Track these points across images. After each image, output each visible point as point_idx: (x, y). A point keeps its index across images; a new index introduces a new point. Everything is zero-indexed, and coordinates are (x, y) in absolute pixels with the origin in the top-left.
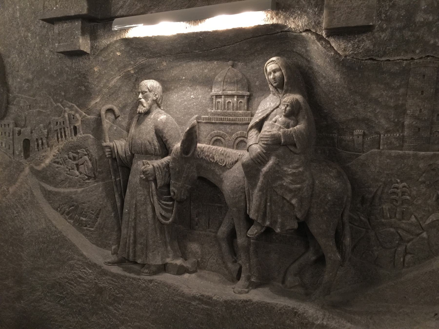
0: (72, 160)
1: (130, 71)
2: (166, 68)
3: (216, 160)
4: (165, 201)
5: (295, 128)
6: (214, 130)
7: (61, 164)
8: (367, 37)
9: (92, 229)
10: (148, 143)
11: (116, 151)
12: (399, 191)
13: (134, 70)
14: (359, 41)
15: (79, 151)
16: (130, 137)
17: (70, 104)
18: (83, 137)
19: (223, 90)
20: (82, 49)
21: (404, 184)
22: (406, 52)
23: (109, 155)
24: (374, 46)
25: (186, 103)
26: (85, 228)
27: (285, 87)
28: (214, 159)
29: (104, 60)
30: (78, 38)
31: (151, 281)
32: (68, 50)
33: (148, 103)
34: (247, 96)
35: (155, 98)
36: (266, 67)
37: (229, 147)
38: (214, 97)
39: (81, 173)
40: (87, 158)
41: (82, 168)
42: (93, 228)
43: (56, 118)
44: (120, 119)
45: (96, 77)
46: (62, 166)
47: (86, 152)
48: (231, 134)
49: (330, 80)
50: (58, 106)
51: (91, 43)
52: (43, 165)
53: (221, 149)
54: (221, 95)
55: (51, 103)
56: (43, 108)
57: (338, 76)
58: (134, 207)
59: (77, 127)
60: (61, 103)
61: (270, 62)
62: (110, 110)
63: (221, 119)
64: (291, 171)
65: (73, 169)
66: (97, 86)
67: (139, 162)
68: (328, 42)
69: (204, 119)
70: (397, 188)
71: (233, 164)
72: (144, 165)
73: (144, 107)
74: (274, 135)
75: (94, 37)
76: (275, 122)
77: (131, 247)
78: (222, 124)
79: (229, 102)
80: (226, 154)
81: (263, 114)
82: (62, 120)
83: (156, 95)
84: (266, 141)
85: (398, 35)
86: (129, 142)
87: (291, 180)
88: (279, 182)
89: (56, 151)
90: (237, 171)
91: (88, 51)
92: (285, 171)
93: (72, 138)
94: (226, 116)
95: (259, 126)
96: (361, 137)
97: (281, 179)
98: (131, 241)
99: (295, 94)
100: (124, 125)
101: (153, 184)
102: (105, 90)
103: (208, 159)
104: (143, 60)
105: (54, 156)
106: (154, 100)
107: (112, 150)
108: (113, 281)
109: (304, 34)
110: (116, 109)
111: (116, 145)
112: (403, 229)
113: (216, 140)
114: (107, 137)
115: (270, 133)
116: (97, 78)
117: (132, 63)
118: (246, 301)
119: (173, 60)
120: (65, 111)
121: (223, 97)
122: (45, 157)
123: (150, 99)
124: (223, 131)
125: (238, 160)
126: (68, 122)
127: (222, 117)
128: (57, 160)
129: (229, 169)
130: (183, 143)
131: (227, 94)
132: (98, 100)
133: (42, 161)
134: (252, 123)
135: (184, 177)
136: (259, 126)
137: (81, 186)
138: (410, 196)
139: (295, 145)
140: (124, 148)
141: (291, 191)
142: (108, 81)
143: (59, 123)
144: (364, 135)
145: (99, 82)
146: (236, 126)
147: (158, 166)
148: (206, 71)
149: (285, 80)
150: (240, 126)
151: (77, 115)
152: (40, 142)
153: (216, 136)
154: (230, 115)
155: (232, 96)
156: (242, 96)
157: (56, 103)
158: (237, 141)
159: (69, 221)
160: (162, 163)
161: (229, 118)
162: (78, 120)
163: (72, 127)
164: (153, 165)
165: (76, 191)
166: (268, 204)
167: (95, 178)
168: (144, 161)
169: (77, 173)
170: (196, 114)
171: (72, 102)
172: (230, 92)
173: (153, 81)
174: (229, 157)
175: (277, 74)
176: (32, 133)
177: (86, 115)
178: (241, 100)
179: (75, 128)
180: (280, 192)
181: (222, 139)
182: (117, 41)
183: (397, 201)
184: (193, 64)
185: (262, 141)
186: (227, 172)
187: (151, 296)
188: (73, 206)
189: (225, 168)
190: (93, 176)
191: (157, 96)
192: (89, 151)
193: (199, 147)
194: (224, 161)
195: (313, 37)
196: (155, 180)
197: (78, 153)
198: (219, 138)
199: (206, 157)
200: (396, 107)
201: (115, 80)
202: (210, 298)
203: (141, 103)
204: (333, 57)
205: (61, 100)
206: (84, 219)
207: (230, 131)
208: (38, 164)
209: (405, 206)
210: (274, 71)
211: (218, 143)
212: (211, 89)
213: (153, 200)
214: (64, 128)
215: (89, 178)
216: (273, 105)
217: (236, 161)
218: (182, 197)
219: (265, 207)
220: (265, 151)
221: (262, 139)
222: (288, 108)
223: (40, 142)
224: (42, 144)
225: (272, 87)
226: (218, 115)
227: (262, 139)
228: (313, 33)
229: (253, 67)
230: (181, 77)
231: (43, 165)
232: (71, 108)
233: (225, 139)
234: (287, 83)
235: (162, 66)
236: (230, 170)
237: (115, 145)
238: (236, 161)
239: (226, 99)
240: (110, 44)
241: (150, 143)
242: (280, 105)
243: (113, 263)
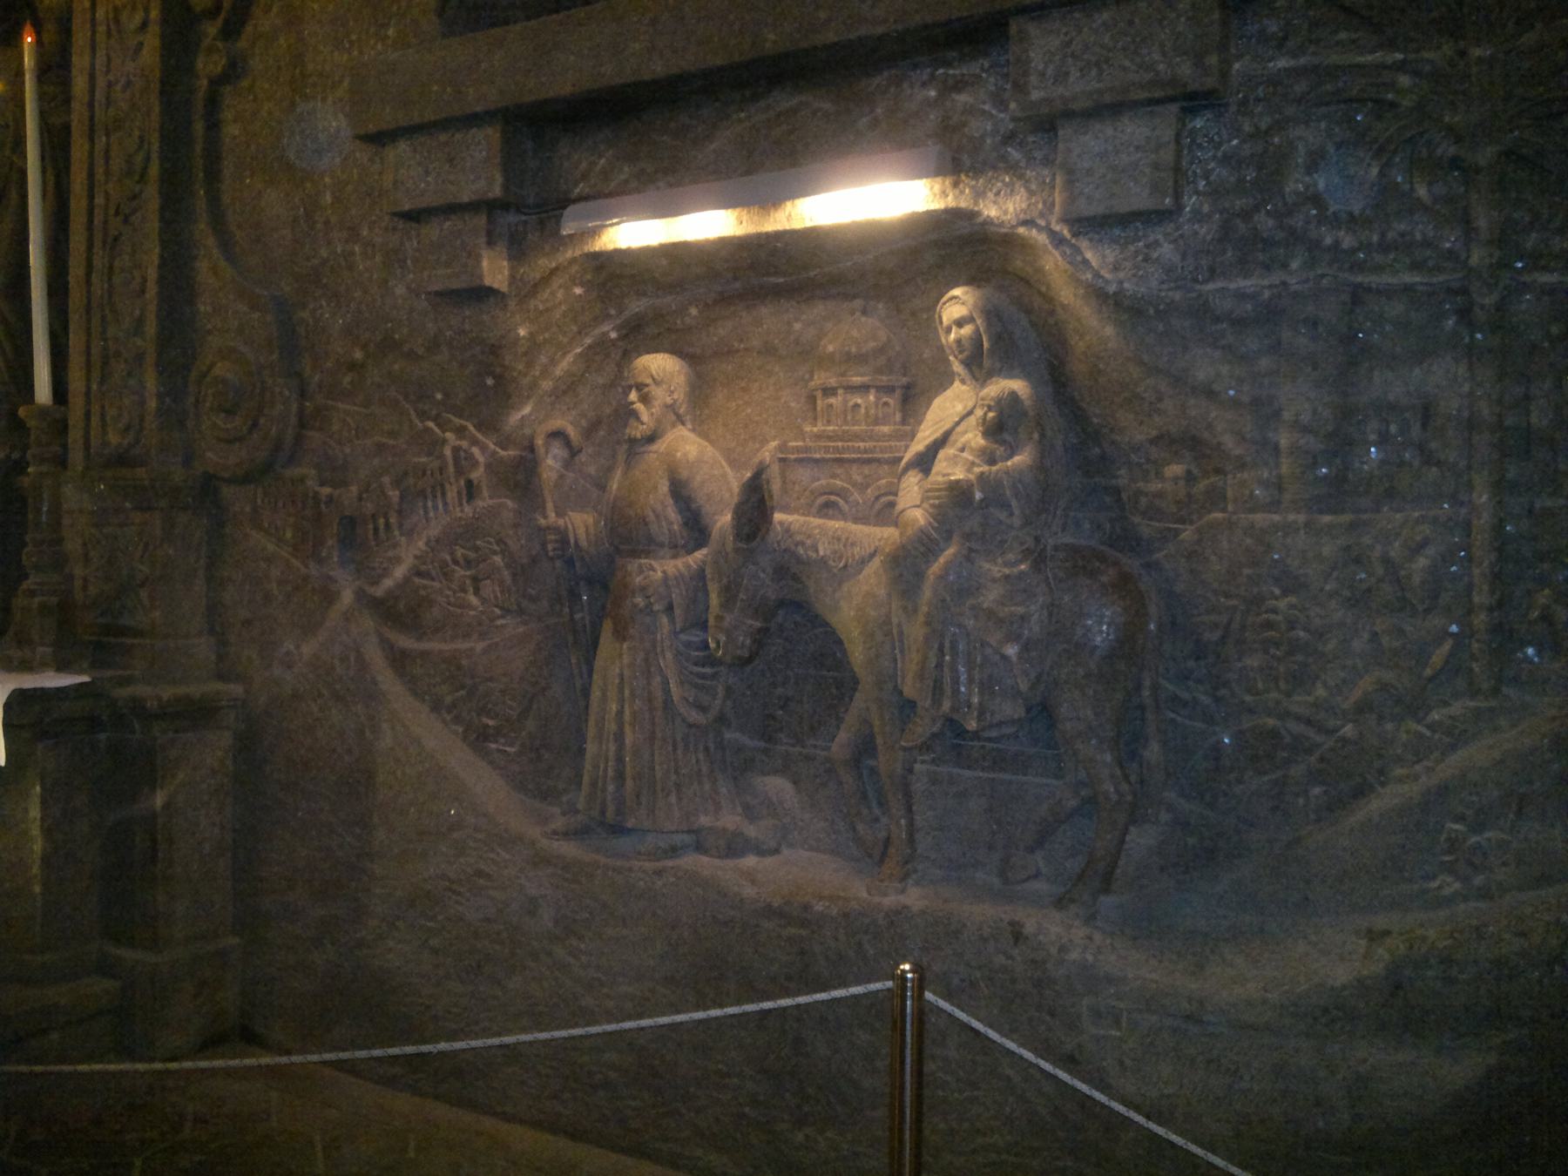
0: (461, 568)
1: (608, 332)
4: (696, 664)
5: (1009, 463)
6: (819, 480)
7: (433, 579)
8: (1166, 235)
9: (513, 750)
10: (651, 514)
13: (618, 331)
14: (1147, 246)
15: (478, 543)
17: (457, 421)
18: (491, 507)
19: (843, 375)
20: (487, 282)
21: (1292, 599)
22: (1267, 268)
23: (554, 549)
24: (1184, 256)
26: (493, 746)
27: (987, 363)
28: (817, 551)
29: (541, 307)
30: (478, 259)
31: (659, 873)
32: (454, 287)
33: (652, 414)
35: (669, 400)
36: (940, 312)
37: (856, 520)
38: (819, 394)
39: (484, 601)
40: (500, 560)
41: (488, 588)
42: (511, 745)
43: (424, 459)
44: (583, 457)
45: (521, 350)
46: (436, 584)
47: (498, 545)
48: (863, 488)
50: (427, 429)
51: (512, 268)
52: (388, 583)
53: (836, 525)
55: (411, 421)
56: (392, 434)
57: (1109, 331)
59: (475, 482)
60: (435, 419)
61: (948, 301)
62: (558, 435)
63: (837, 450)
64: (1000, 571)
65: (464, 590)
66: (525, 375)
68: (1078, 250)
69: (798, 450)
72: (641, 571)
73: (643, 423)
74: (958, 482)
75: (518, 250)
76: (962, 450)
77: (611, 788)
78: (840, 461)
79: (857, 406)
80: (847, 539)
81: (935, 431)
82: (436, 464)
83: (672, 392)
84: (938, 498)
85: (1242, 227)
88: (971, 601)
89: (421, 544)
91: (504, 288)
93: (462, 511)
94: (850, 440)
95: (924, 462)
96: (1182, 483)
98: (610, 773)
99: (1011, 377)
100: (593, 473)
101: (665, 620)
102: (547, 385)
103: (802, 552)
104: (638, 303)
105: (416, 557)
106: (667, 406)
109: (1021, 230)
110: (572, 432)
111: (572, 524)
112: (1298, 718)
113: (827, 505)
114: (550, 505)
116: (525, 354)
117: (613, 312)
120: (444, 441)
121: (840, 391)
122: (398, 560)
123: (656, 403)
124: (841, 480)
125: (875, 551)
126: (451, 469)
127: (840, 444)
128: (423, 568)
130: (739, 513)
131: (850, 384)
132: (527, 410)
133: (386, 573)
134: (908, 457)
135: (742, 600)
136: (924, 462)
137: (483, 636)
138: (1305, 629)
139: (1005, 506)
140: (592, 531)
142: (553, 362)
143: (429, 472)
144: (1190, 478)
145: (530, 365)
146: (874, 465)
147: (677, 574)
148: (797, 326)
149: (986, 345)
150: (886, 467)
151: (475, 451)
152: (382, 521)
153: (825, 493)
154: (857, 437)
155: (864, 389)
156: (890, 390)
157: (422, 422)
158: (878, 506)
159: (454, 727)
160: (688, 566)
161: (856, 445)
162: (477, 462)
163: (462, 483)
164: (664, 572)
165: (472, 649)
166: (947, 658)
167: (521, 611)
169: (474, 600)
170: (774, 438)
171: (461, 417)
172: (857, 380)
173: (666, 356)
174: (853, 544)
175: (967, 330)
176: (360, 499)
177: (498, 450)
178: (885, 399)
179: (469, 483)
181: (841, 502)
182: (573, 261)
183: (1277, 645)
185: (929, 498)
188: (463, 687)
190: (515, 607)
191: (676, 396)
192: (505, 544)
193: (781, 523)
194: (840, 558)
197: (476, 549)
198: (833, 498)
199: (797, 545)
200: (1256, 402)
201: (570, 358)
203: (634, 414)
205: (434, 412)
206: (491, 723)
207: (859, 479)
208: (375, 582)
209: (1300, 658)
210: (960, 323)
211: (831, 512)
214: (442, 486)
215: (507, 611)
216: (959, 408)
217: (872, 555)
220: (936, 525)
221: (930, 494)
222: (991, 415)
223: (382, 521)
224: (387, 525)
226: (830, 438)
227: (930, 494)
228: (1040, 229)
230: (736, 344)
231: (388, 583)
232: (460, 432)
233: (847, 502)
234: (989, 350)
237: (570, 526)
238: (872, 555)
239: (849, 396)
240: (557, 269)
241: (657, 516)
242: (975, 407)
243: (566, 835)
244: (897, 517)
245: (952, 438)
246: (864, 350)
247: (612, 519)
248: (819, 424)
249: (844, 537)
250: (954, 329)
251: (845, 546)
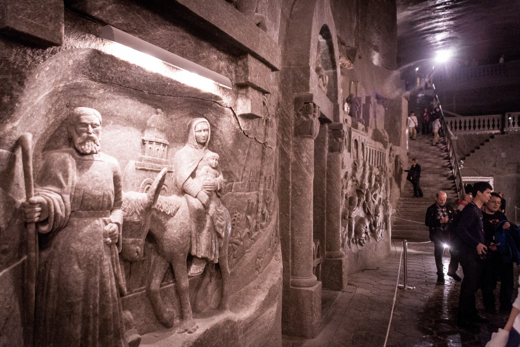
2: (100, 98)
12: (236, 218)
16: (72, 187)
25: (119, 145)
49: (224, 143)
54: (153, 142)
58: (98, 285)
67: (97, 222)
70: (235, 217)
78: (151, 171)
84: (210, 188)
86: (71, 195)
90: (182, 218)
107: (46, 207)
119: (114, 91)
121: (154, 143)
148: (139, 112)
168: (104, 218)
184: (130, 101)
185: (205, 188)
186: (170, 220)
189: (170, 216)
195: (232, 113)
204: (237, 129)
212: (143, 132)
213: (118, 269)
229: (171, 120)
235: (96, 94)
236: (174, 217)
238: (178, 208)
245: (199, 167)
248: (146, 154)
250: (203, 131)
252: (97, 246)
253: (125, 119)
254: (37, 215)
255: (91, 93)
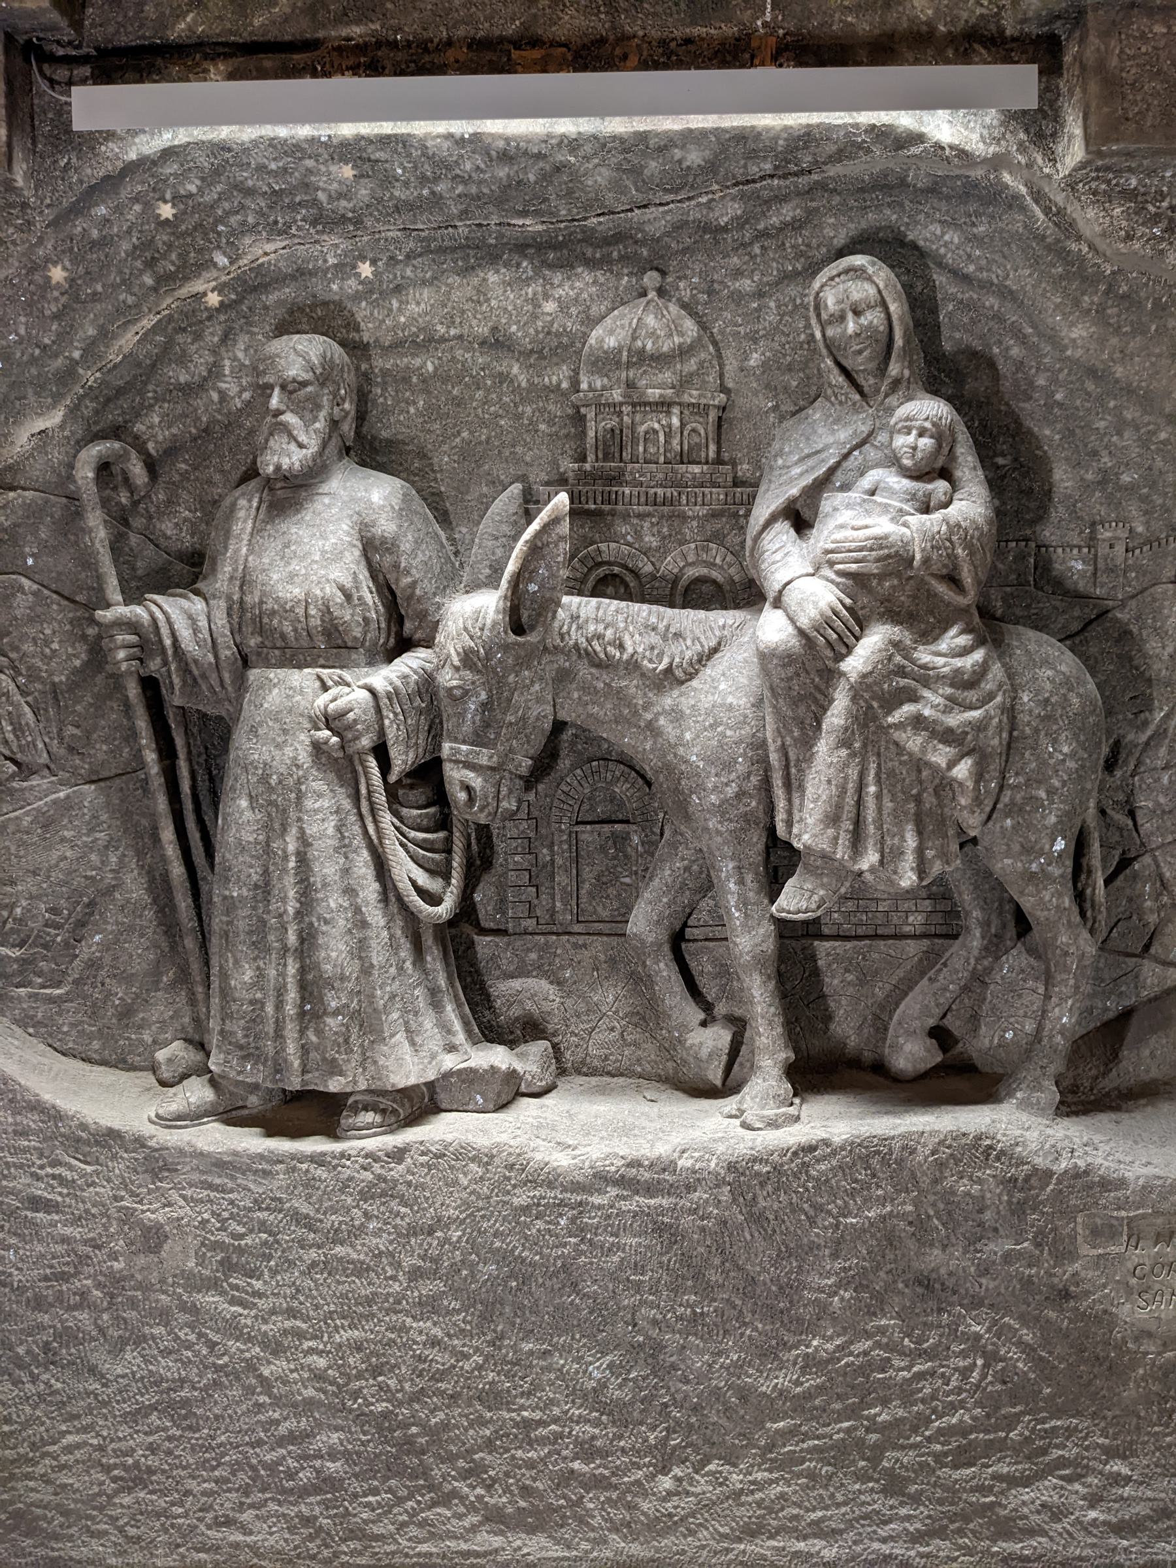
3: (630, 650)
5: (953, 510)
11: (168, 642)
28: (621, 647)
34: (718, 407)
71: (700, 661)
72: (325, 688)
73: (301, 446)
76: (873, 493)
80: (667, 628)
86: (229, 598)
87: (949, 698)
88: (908, 709)
92: (924, 667)
97: (914, 698)
101: (372, 763)
103: (598, 648)
108: (211, 1187)
111: (164, 612)
115: (861, 534)
118: (812, 1148)
125: (719, 644)
129: (682, 683)
141: (947, 736)
148: (550, 307)
149: (899, 341)
160: (406, 677)
166: (872, 789)
168: (325, 672)
180: (914, 742)
187: (403, 1210)
189: (673, 678)
194: (660, 656)
196: (381, 752)
202: (669, 1166)
211: (610, 590)
213: (378, 830)
218: (505, 804)
219: (859, 802)
220: (848, 601)
225: (836, 371)
238: (715, 650)
244: (780, 592)
246: (665, 349)
247: (241, 602)
249: (661, 626)
251: (665, 638)
252: (289, 751)
253: (483, 343)
254: (121, 654)
255: (335, 287)
